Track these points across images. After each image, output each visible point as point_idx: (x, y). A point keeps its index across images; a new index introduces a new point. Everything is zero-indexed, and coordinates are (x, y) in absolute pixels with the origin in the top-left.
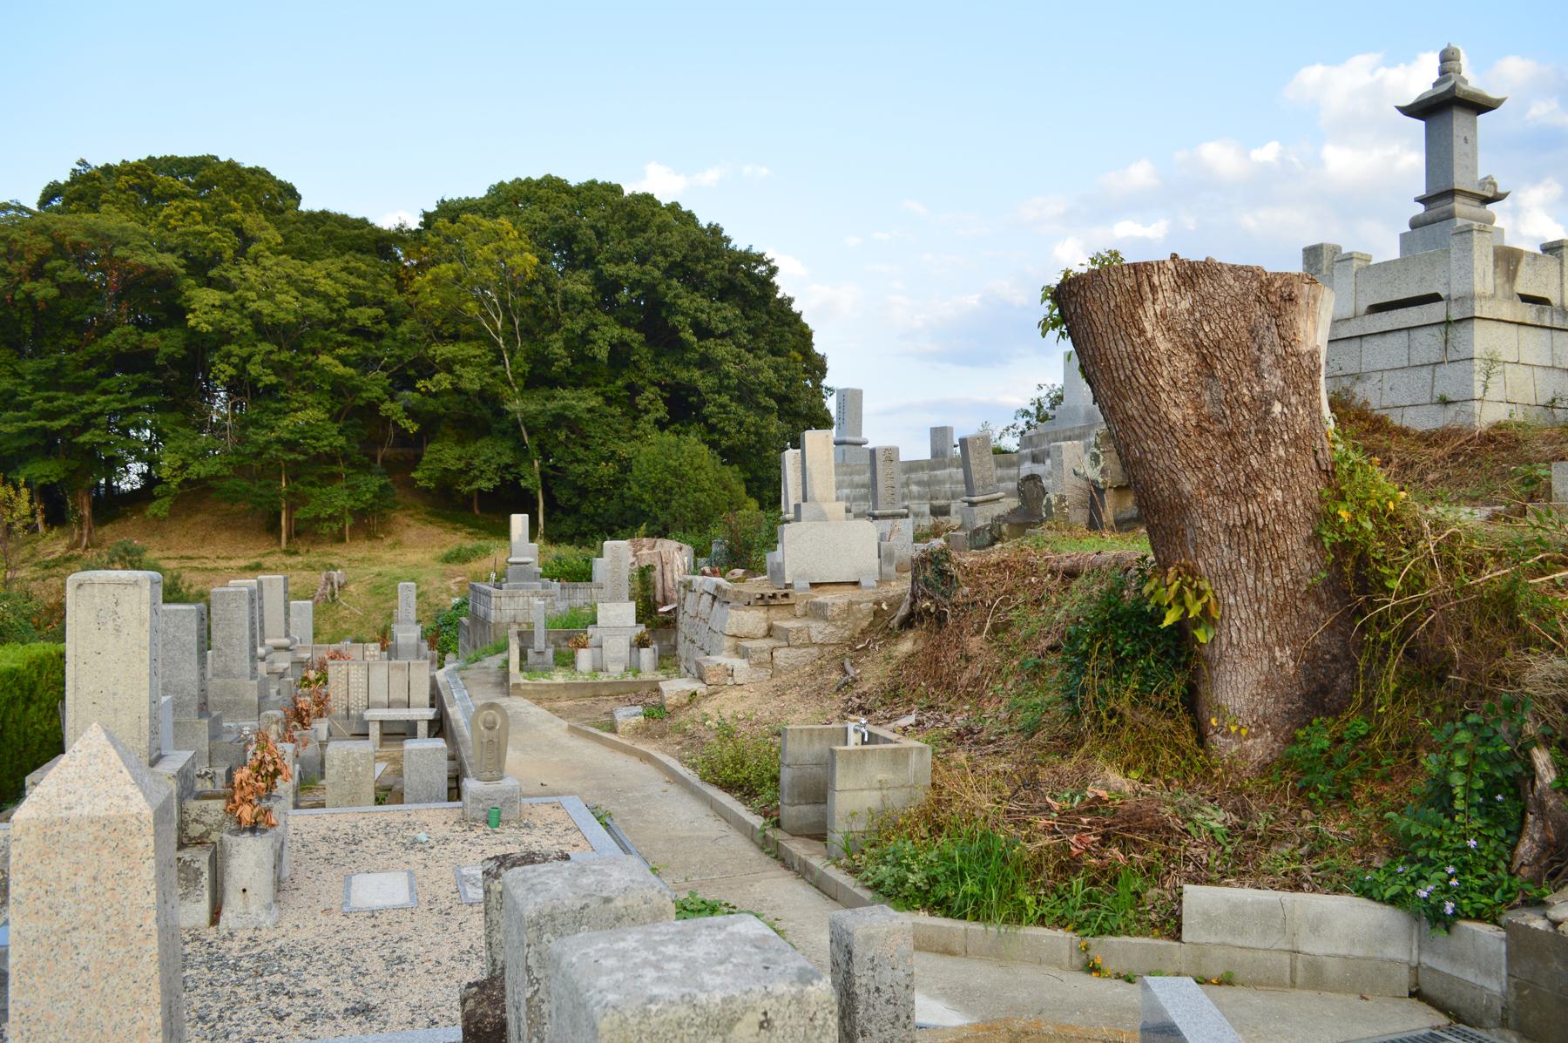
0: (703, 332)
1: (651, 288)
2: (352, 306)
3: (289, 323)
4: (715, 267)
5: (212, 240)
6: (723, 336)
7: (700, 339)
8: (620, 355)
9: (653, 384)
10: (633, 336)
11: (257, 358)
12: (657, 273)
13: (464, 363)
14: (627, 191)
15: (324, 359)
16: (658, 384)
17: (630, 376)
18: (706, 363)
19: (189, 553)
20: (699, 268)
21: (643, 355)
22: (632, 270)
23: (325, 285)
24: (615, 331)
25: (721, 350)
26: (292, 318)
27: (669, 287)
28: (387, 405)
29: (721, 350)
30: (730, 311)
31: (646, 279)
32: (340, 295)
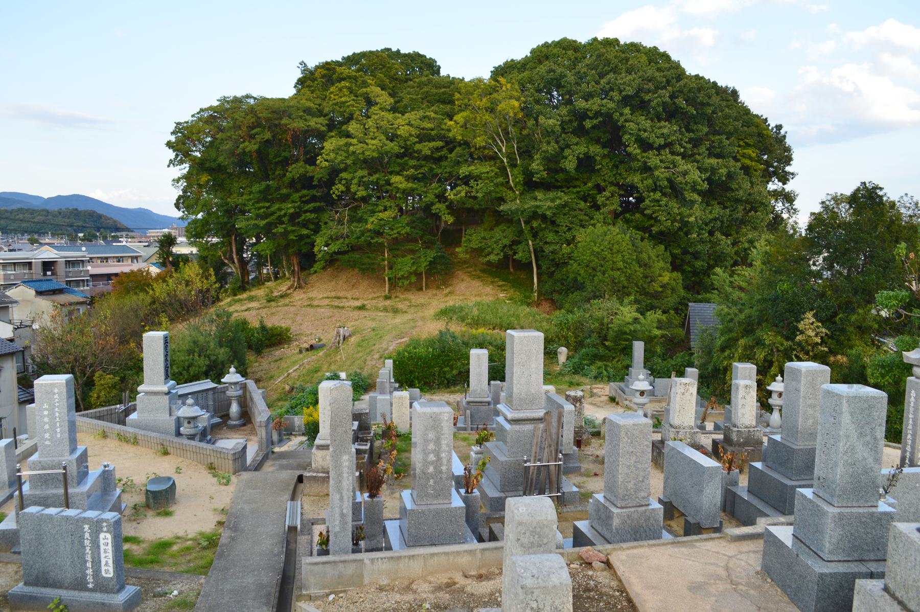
0: (645, 146)
1: (608, 116)
2: (420, 142)
3: (373, 158)
4: (660, 97)
5: (348, 107)
6: (660, 148)
7: (644, 151)
8: (586, 164)
9: (612, 183)
10: (596, 150)
11: (355, 181)
12: (611, 105)
13: (477, 178)
14: (467, 80)
15: (395, 179)
16: (617, 185)
17: (596, 180)
18: (647, 169)
19: (341, 294)
20: (647, 98)
21: (604, 166)
22: (594, 104)
23: (403, 131)
24: (582, 149)
25: (653, 159)
26: (375, 155)
27: (621, 115)
28: (438, 205)
29: (653, 159)
30: (667, 128)
31: (604, 110)
32: (411, 135)
